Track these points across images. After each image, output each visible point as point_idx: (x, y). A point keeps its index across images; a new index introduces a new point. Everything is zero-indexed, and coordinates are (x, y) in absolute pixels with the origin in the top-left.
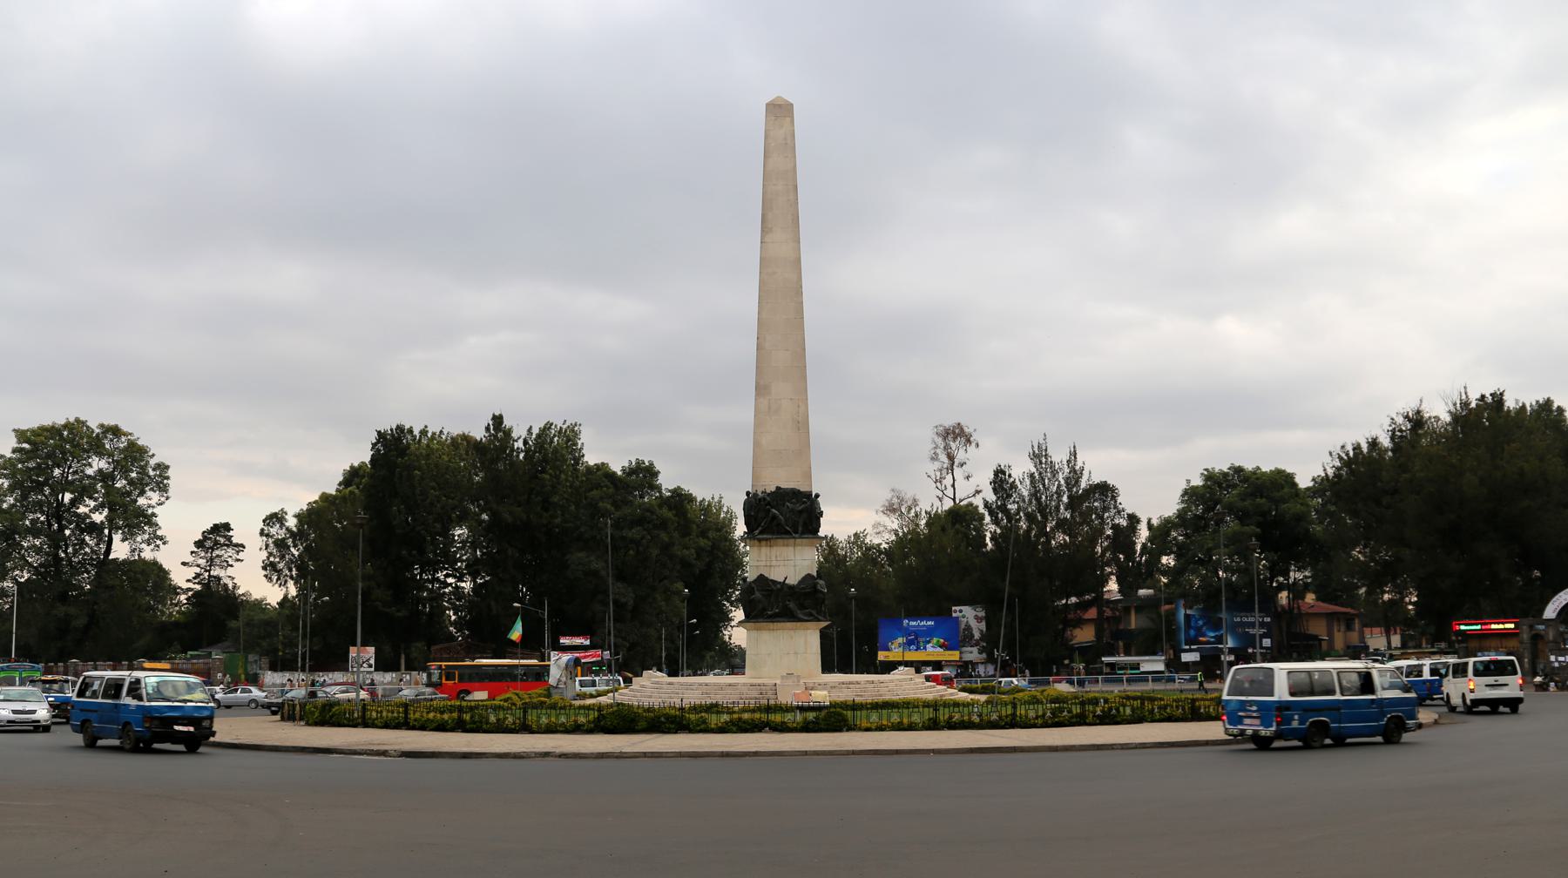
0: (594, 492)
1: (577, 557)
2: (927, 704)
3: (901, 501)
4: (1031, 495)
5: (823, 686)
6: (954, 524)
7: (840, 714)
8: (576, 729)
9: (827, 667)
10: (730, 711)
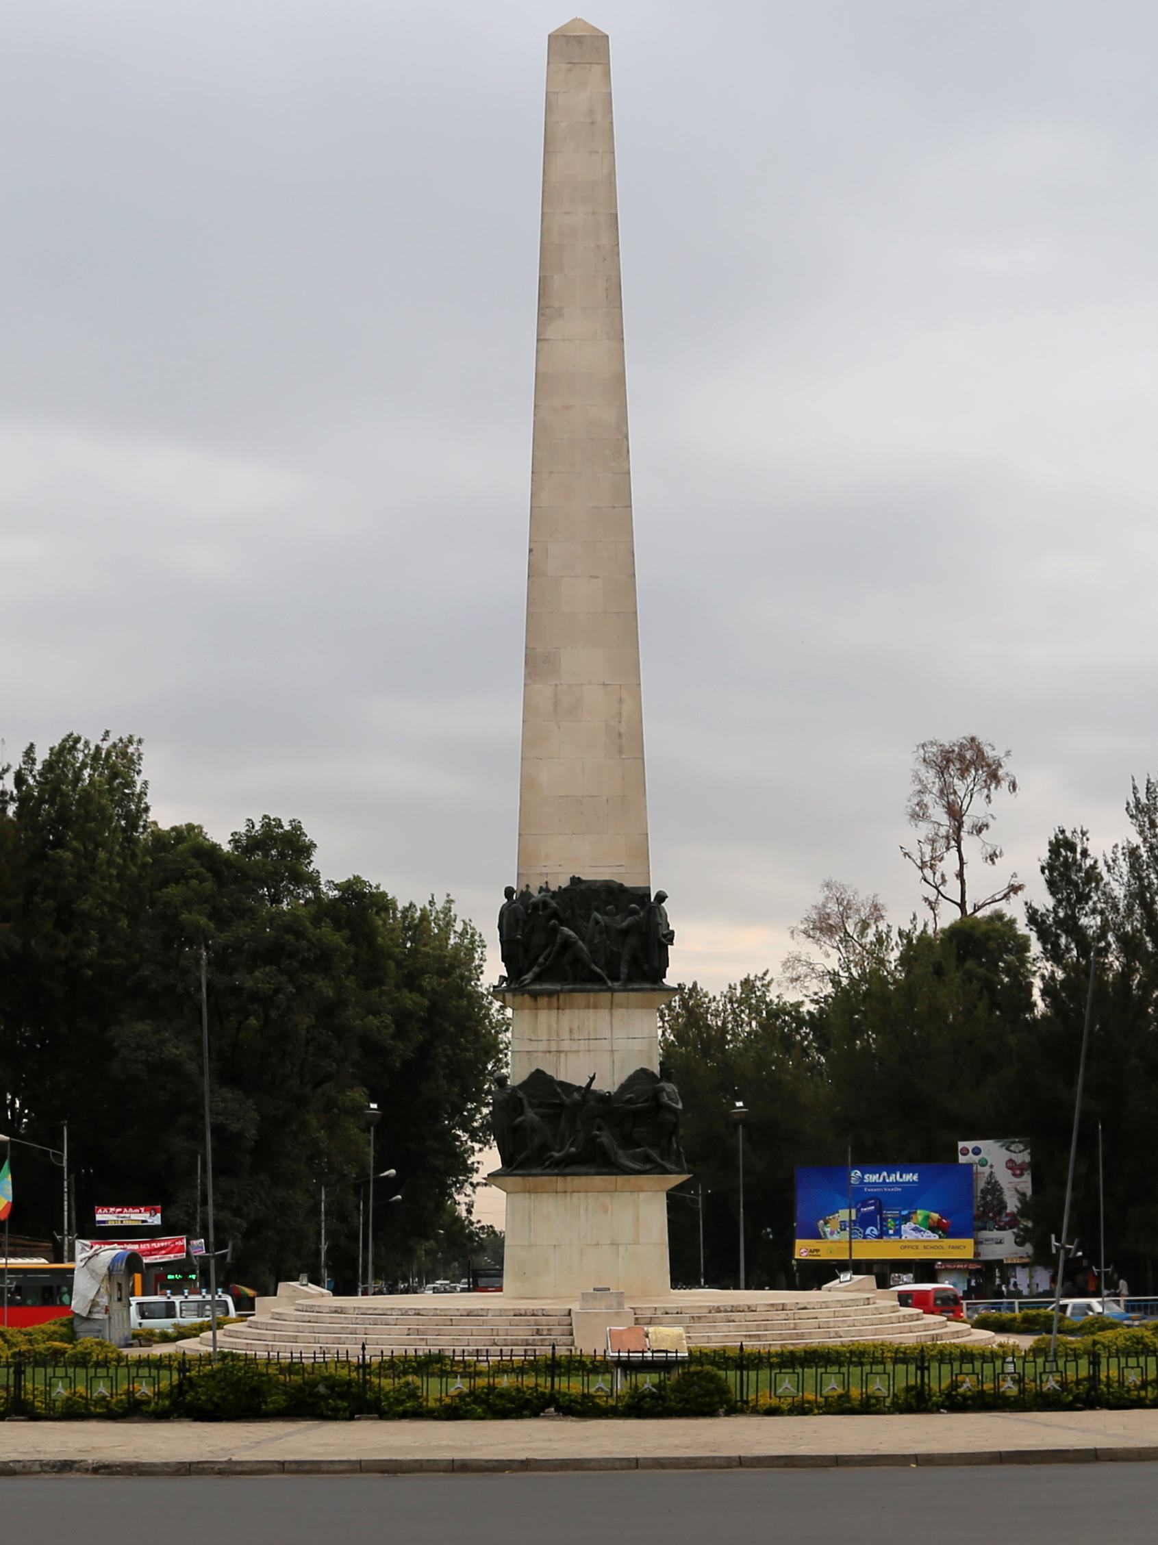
0: (172, 890)
1: (134, 1032)
2: (902, 1356)
3: (847, 908)
4: (1131, 895)
5: (675, 1316)
6: (961, 960)
7: (712, 1378)
8: (132, 1410)
9: (683, 1276)
10: (469, 1371)
